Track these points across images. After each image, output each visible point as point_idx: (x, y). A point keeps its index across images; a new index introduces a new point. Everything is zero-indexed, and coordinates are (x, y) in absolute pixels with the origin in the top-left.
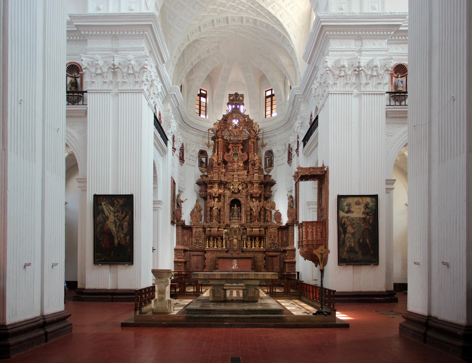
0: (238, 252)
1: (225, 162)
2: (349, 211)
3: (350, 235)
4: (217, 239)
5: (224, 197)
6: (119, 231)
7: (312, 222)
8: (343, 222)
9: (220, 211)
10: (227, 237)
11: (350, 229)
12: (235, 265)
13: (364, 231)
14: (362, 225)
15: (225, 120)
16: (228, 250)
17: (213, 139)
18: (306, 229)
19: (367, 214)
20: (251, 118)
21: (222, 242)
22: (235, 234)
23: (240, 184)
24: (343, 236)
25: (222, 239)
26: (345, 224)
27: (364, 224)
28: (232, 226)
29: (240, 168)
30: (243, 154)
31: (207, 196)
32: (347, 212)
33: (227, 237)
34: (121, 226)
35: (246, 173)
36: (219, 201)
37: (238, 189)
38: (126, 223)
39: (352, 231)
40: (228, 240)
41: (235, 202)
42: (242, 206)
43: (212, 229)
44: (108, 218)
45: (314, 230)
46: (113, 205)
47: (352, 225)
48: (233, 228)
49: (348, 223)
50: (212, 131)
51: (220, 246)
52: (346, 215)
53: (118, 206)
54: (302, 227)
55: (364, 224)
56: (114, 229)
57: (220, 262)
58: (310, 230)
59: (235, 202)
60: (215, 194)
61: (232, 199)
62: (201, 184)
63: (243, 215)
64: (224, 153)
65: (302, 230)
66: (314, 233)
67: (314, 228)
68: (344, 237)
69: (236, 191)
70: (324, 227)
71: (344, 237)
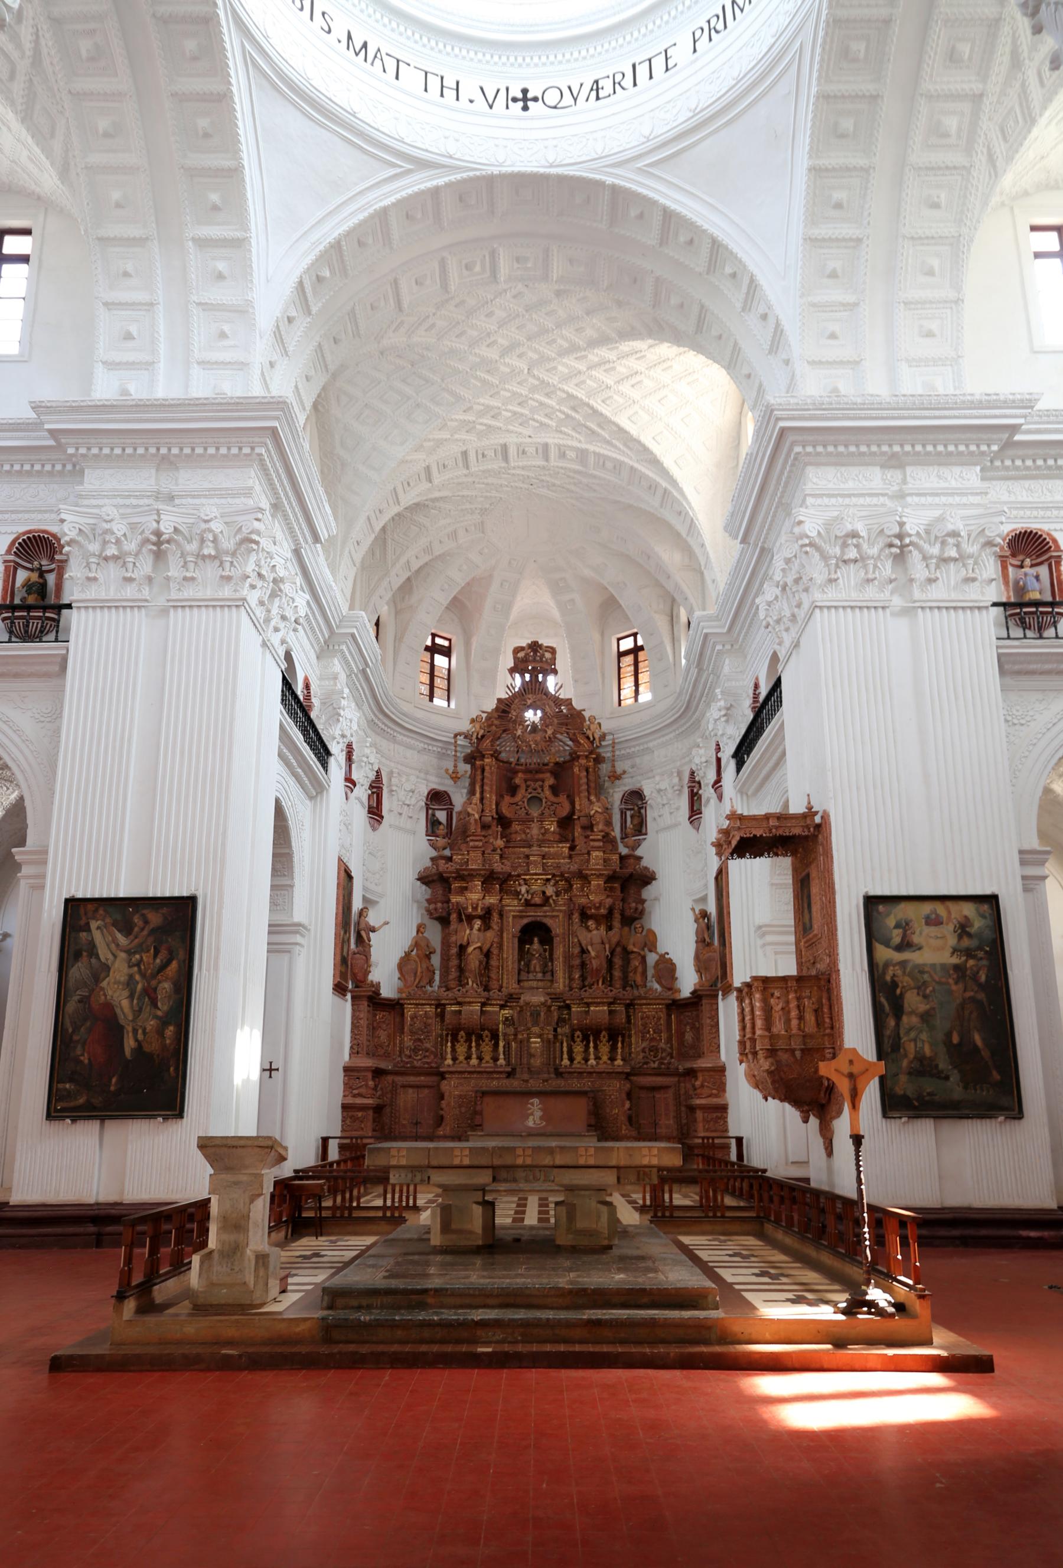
0: (546, 1076)
1: (503, 822)
2: (905, 945)
3: (915, 1020)
4: (480, 1038)
6: (140, 1010)
7: (785, 979)
8: (888, 978)
9: (488, 955)
11: (912, 1000)
12: (534, 1114)
13: (962, 1006)
14: (954, 987)
15: (504, 711)
16: (514, 1069)
17: (470, 759)
18: (765, 1001)
19: (969, 953)
20: (577, 705)
21: (496, 1045)
22: (536, 1023)
23: (548, 880)
24: (892, 1023)
25: (495, 1036)
26: (894, 984)
27: (961, 986)
28: (525, 998)
29: (547, 836)
30: (555, 800)
31: (449, 914)
32: (899, 948)
33: (511, 1030)
34: (150, 994)
35: (566, 850)
36: (486, 926)
37: (544, 893)
38: (167, 986)
39: (923, 1007)
40: (515, 1039)
41: (535, 932)
42: (556, 940)
43: (465, 1008)
44: (107, 968)
45: (793, 1004)
46: (127, 929)
47: (921, 987)
48: (527, 1004)
49: (905, 981)
50: (466, 737)
51: (487, 1057)
52: (898, 957)
53: (145, 932)
54: (750, 995)
55: (961, 986)
56: (125, 1003)
57: (489, 1105)
58: (777, 1005)
59: (535, 932)
60: (475, 909)
61: (525, 921)
63: (559, 967)
64: (502, 796)
65: (751, 1003)
66: (794, 1013)
67: (791, 996)
68: (898, 1025)
69: (537, 900)
70: (825, 995)
71: (898, 1025)
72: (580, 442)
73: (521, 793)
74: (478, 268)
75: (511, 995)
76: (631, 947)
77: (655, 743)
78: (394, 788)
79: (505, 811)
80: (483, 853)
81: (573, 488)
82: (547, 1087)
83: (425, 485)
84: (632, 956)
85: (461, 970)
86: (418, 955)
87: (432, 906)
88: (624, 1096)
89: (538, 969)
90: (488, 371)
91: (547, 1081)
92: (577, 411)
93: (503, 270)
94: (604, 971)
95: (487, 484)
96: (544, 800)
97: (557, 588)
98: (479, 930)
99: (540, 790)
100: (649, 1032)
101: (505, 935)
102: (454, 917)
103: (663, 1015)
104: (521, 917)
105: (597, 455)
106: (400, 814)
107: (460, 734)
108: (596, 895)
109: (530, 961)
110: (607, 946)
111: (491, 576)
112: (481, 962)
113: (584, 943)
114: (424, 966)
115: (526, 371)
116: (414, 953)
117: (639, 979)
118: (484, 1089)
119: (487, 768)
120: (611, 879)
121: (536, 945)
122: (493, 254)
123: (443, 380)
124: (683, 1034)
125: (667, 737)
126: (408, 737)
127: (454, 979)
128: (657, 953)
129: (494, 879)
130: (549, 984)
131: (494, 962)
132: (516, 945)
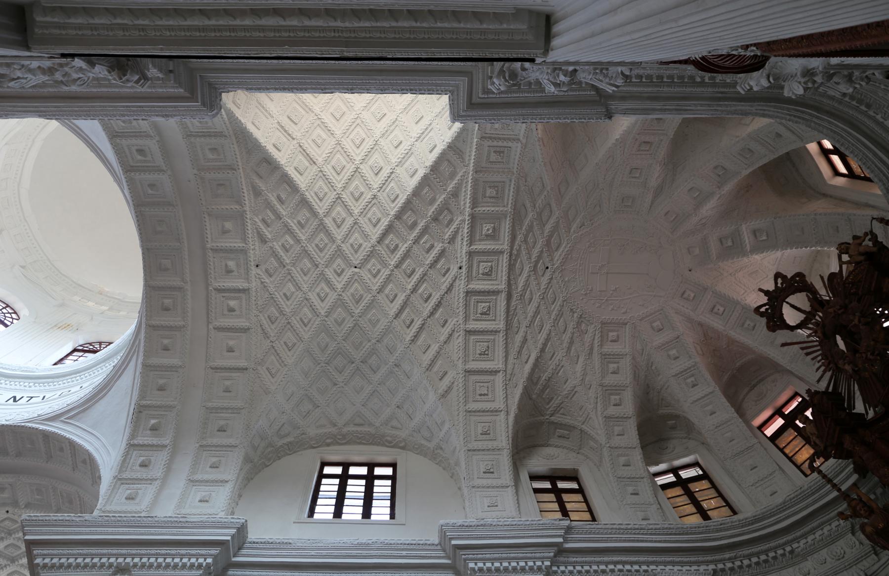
72: (464, 221)
74: (232, 303)
81: (548, 228)
83: (499, 379)
90: (357, 302)
92: (415, 224)
93: (240, 284)
95: (537, 312)
97: (733, 248)
105: (474, 204)
111: (701, 324)
115: (357, 270)
122: (219, 290)
123: (369, 341)
126: (812, 531)
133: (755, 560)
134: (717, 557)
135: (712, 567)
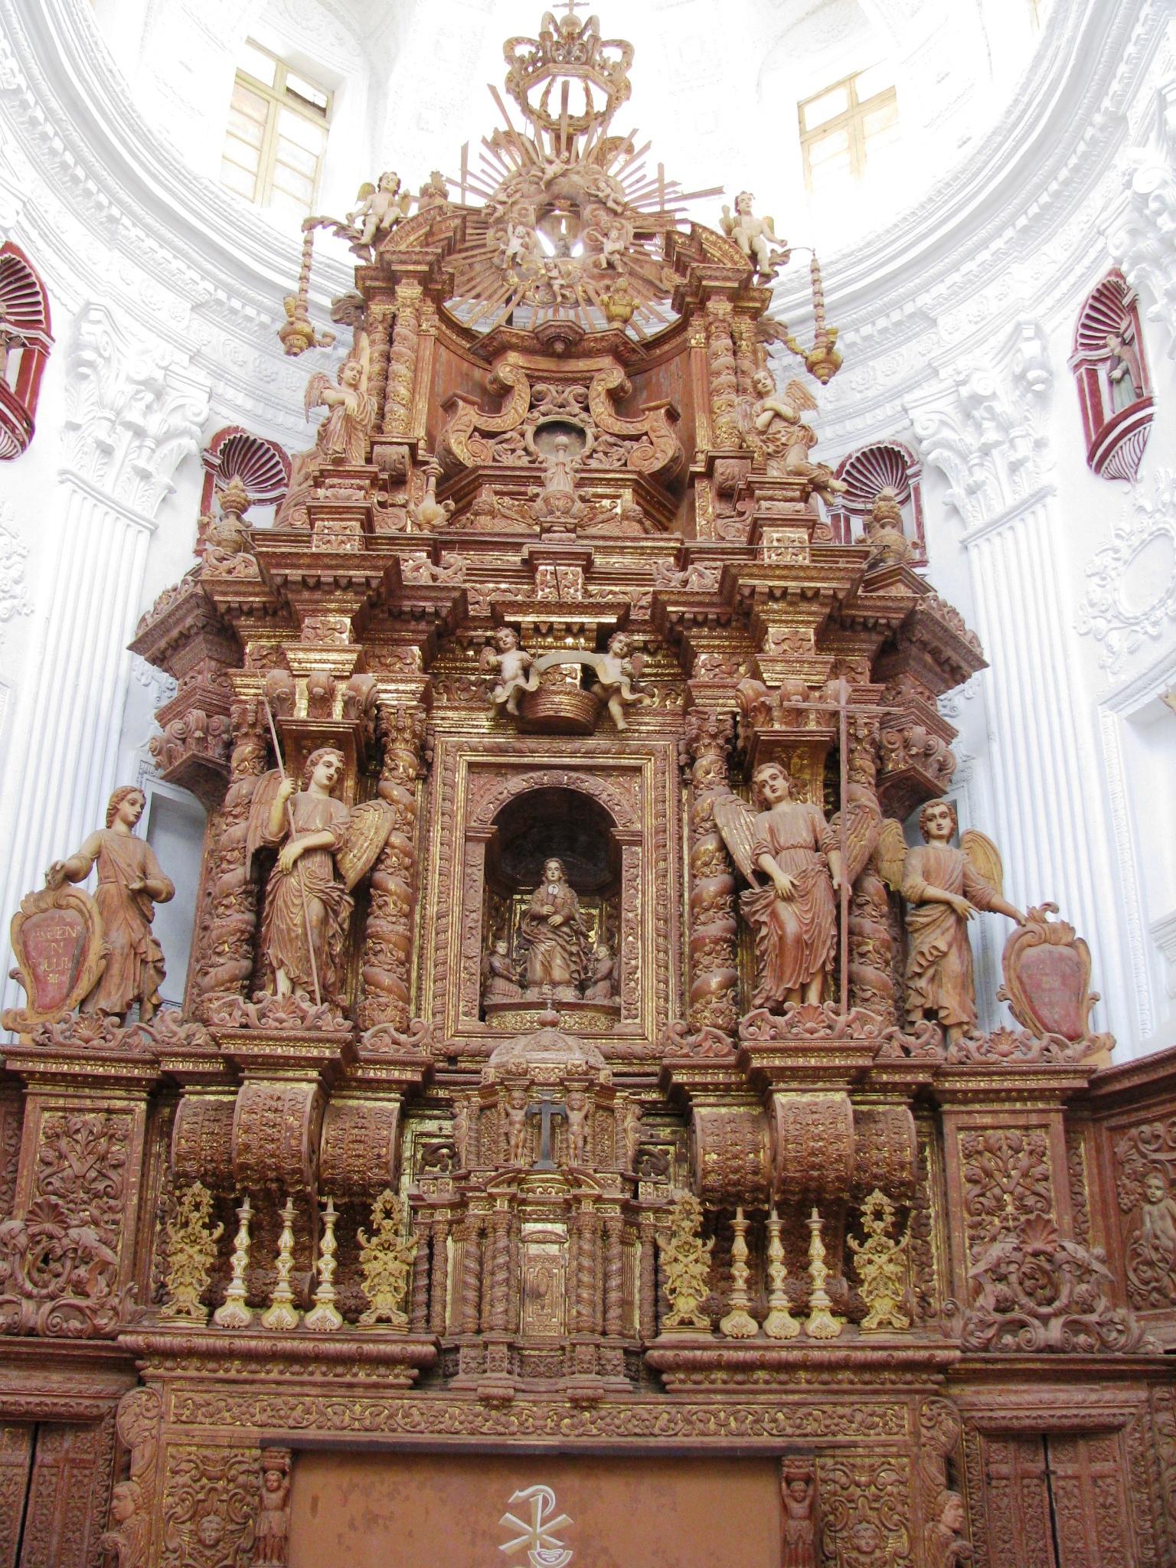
0: (585, 1382)
5: (423, 752)
9: (364, 891)
10: (443, 1190)
28: (510, 1053)
37: (589, 675)
41: (552, 838)
43: (255, 1089)
48: (510, 1078)
59: (552, 838)
60: (321, 701)
61: (517, 784)
62: (185, 637)
64: (450, 406)
69: (564, 704)
73: (517, 407)
75: (452, 1059)
76: (915, 884)
77: (941, 289)
78: (88, 355)
79: (463, 451)
80: (368, 525)
82: (591, 1432)
84: (920, 918)
85: (254, 940)
86: (101, 900)
87: (177, 725)
88: (934, 1470)
89: (558, 974)
91: (593, 1403)
94: (825, 953)
96: (590, 432)
98: (333, 789)
99: (576, 408)
100: (1001, 1205)
101: (436, 834)
102: (246, 749)
103: (1051, 1139)
104: (500, 769)
106: (106, 451)
107: (323, 222)
108: (791, 673)
109: (529, 943)
110: (835, 858)
112: (329, 907)
113: (742, 853)
114: (120, 939)
116: (89, 886)
117: (949, 1001)
118: (312, 1433)
119: (406, 315)
120: (838, 626)
121: (554, 889)
124: (1129, 1214)
125: (985, 255)
127: (226, 985)
128: (1008, 913)
129: (398, 616)
130: (602, 1022)
131: (385, 924)
132: (479, 875)
133: (69, 158)
134: (45, 87)
135: (21, 80)
